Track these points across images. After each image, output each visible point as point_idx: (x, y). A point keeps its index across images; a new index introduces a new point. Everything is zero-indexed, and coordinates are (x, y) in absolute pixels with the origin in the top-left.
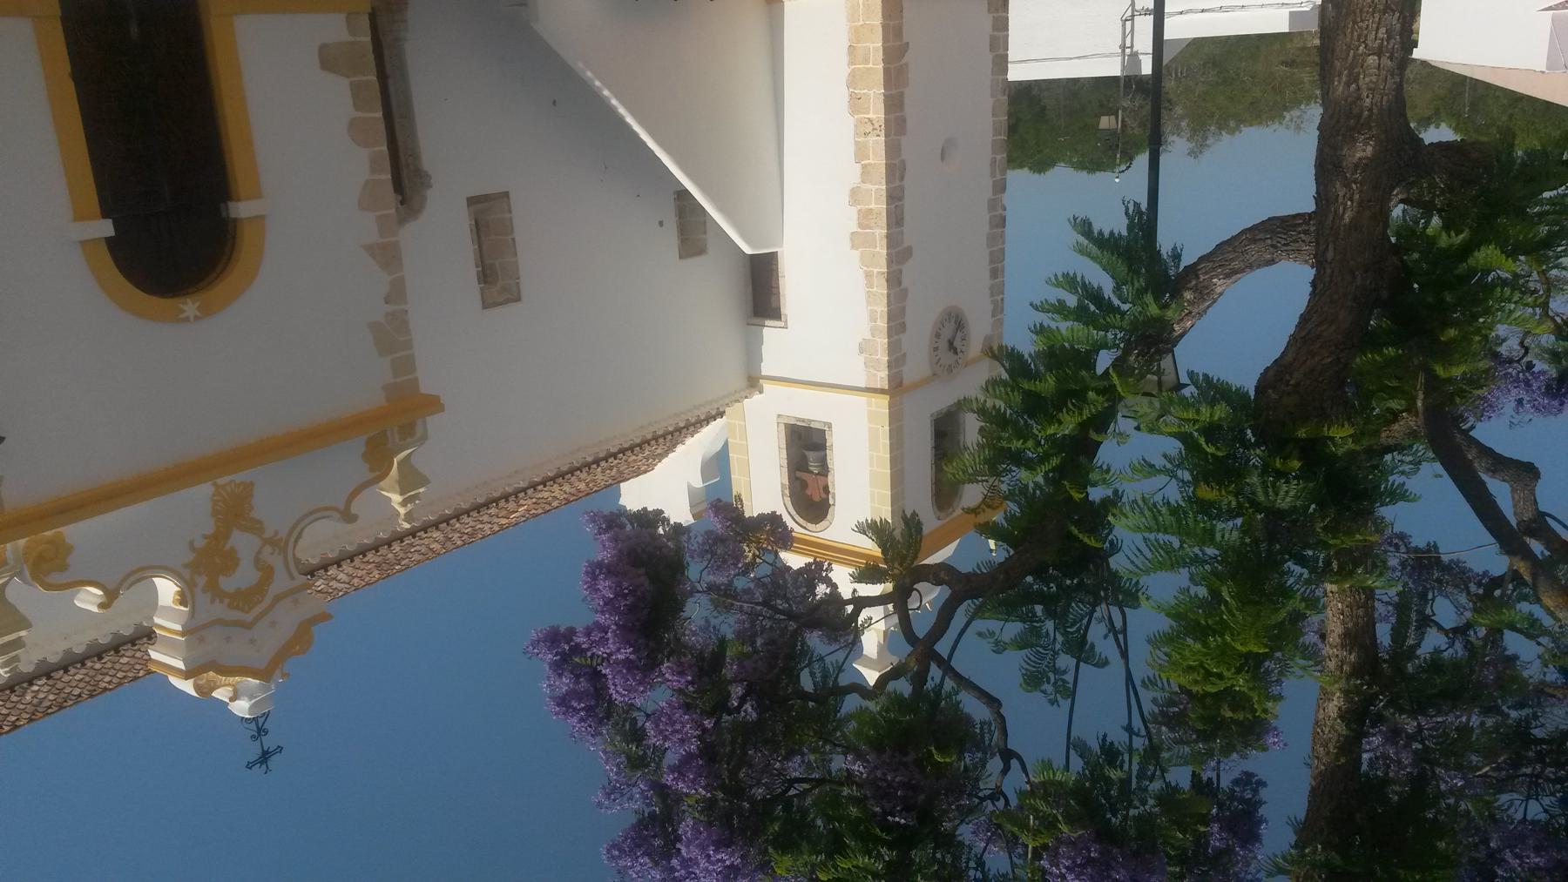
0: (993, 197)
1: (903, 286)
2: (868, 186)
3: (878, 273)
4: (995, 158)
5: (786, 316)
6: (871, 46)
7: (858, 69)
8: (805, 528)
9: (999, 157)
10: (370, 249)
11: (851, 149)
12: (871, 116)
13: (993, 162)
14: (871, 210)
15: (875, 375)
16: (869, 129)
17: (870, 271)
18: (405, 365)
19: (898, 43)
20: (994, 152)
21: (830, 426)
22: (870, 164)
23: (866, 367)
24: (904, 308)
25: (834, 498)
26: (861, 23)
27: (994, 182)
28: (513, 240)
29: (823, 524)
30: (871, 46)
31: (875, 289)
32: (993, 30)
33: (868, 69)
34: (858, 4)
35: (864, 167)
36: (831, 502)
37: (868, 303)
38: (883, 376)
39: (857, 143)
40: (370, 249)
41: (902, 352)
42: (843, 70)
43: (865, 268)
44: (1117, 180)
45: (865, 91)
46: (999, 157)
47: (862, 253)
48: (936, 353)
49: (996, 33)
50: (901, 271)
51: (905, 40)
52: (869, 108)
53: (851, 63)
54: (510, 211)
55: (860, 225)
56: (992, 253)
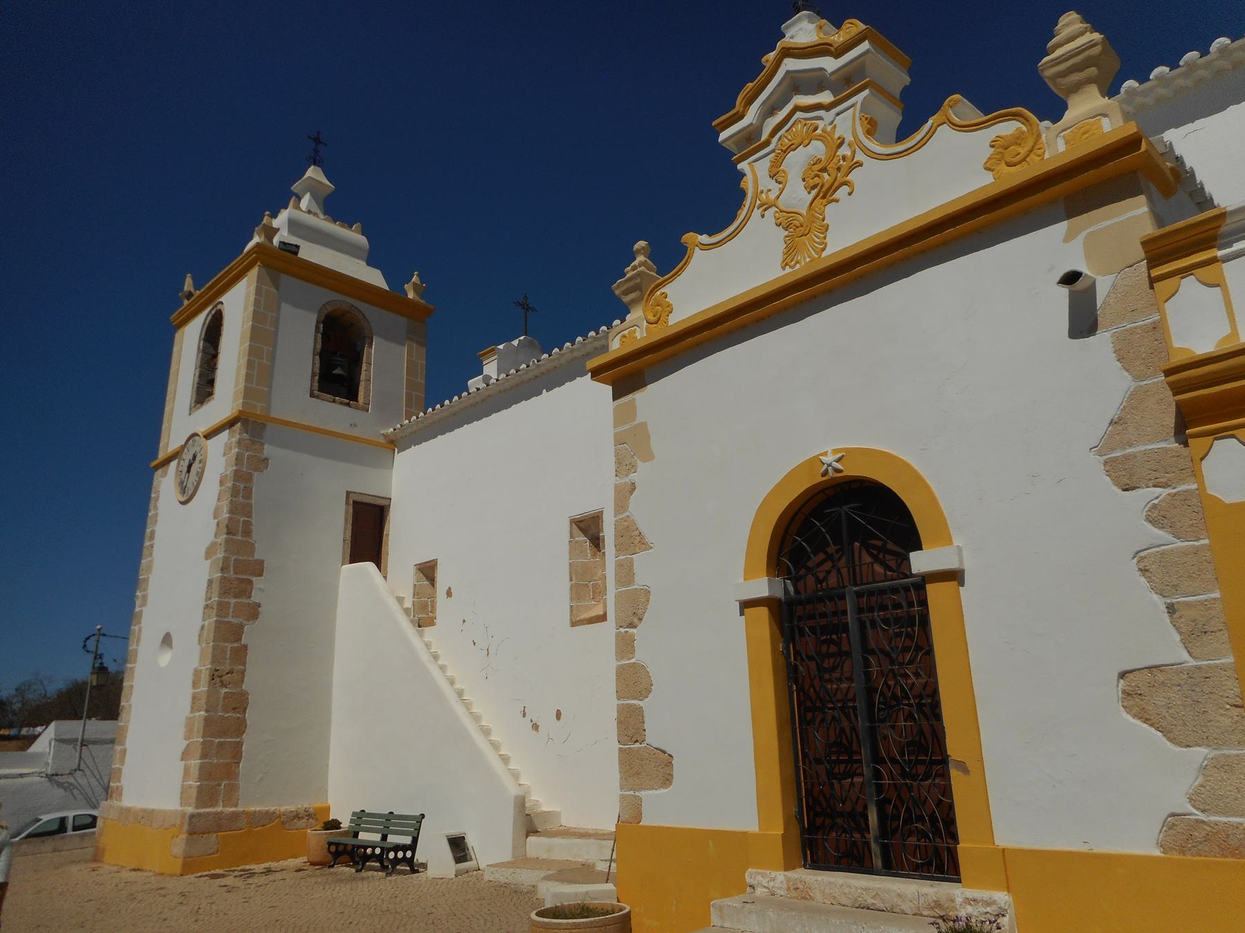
1: (216, 521)
2: (235, 621)
10: (644, 545)
11: (251, 657)
12: (224, 690)
14: (235, 597)
16: (226, 678)
18: (620, 418)
19: (188, 762)
21: (312, 395)
25: (317, 328)
27: (140, 623)
28: (571, 580)
31: (242, 519)
37: (250, 506)
39: (244, 664)
40: (644, 545)
41: (225, 457)
42: (249, 741)
44: (98, 627)
47: (253, 556)
51: (183, 762)
53: (239, 744)
54: (571, 607)
55: (250, 582)
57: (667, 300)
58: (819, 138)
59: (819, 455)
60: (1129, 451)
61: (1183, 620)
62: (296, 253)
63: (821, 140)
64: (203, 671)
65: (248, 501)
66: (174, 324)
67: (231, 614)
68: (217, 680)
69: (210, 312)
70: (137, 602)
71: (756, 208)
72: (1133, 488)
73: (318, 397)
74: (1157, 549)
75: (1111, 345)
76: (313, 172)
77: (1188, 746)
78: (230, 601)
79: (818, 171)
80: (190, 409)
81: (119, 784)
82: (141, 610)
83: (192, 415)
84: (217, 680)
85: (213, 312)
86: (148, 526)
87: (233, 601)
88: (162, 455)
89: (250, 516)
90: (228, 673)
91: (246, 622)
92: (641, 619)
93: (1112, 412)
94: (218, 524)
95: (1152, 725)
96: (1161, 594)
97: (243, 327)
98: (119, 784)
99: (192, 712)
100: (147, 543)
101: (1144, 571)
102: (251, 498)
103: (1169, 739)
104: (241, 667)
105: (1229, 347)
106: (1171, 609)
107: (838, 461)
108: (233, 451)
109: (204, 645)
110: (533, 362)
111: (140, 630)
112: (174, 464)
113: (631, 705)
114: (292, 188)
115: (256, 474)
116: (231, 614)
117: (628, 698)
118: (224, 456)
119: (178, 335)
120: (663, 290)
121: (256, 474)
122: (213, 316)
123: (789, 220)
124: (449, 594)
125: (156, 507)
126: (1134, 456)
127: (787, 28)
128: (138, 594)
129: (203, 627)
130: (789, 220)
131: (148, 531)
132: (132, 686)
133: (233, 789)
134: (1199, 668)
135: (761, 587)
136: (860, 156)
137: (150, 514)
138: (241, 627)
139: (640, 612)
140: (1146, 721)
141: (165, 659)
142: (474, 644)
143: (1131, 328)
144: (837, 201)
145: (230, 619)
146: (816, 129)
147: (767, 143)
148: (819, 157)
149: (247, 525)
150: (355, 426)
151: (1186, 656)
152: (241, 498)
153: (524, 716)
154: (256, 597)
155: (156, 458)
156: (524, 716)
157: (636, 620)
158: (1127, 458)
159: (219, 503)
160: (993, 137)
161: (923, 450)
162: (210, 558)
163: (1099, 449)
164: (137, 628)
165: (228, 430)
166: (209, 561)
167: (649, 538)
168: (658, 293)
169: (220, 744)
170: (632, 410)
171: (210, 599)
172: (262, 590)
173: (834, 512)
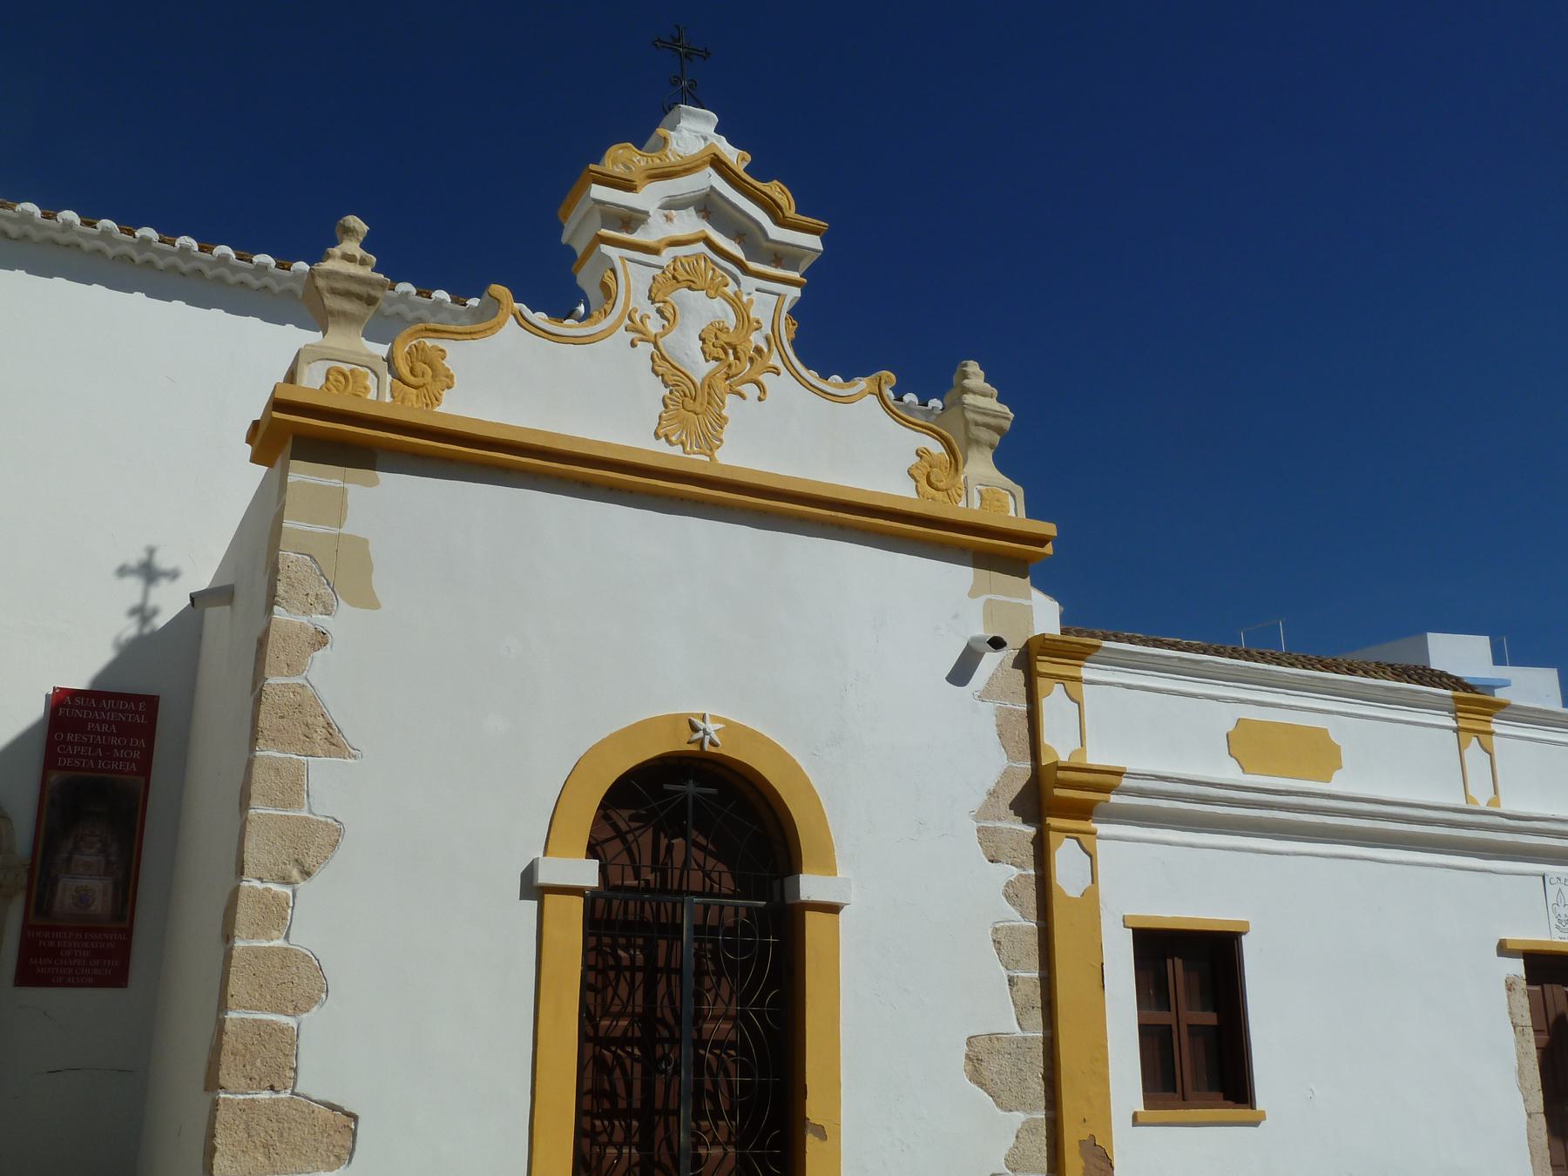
57: (444, 362)
58: (726, 298)
59: (692, 715)
60: (998, 824)
61: (1019, 993)
63: (732, 306)
71: (622, 328)
72: (997, 861)
74: (1007, 924)
75: (994, 718)
77: (1011, 1111)
79: (726, 343)
92: (306, 874)
93: (991, 785)
95: (986, 1090)
96: (1006, 967)
101: (997, 942)
103: (998, 1105)
105: (1075, 762)
106: (1011, 981)
107: (717, 731)
113: (268, 1023)
117: (259, 1009)
120: (441, 344)
123: (676, 378)
126: (1001, 831)
127: (689, 113)
130: (676, 378)
134: (1025, 1039)
135: (588, 874)
136: (775, 360)
139: (309, 862)
140: (981, 1085)
143: (1010, 709)
144: (742, 396)
146: (726, 285)
147: (655, 251)
148: (727, 325)
151: (1017, 1028)
157: (295, 873)
158: (996, 830)
160: (920, 446)
161: (815, 755)
163: (980, 815)
167: (351, 735)
168: (429, 343)
170: (337, 508)
173: (676, 792)
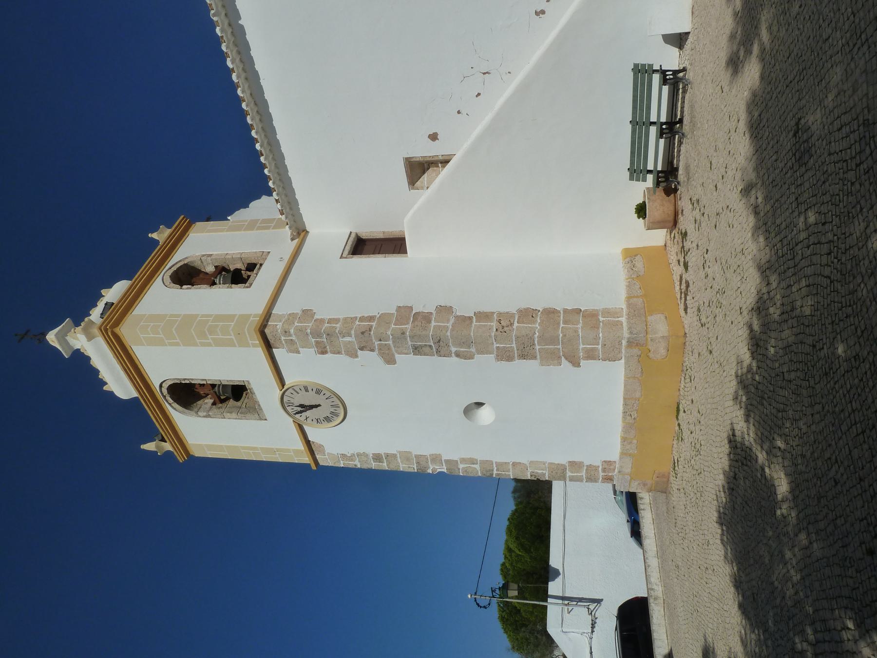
0: (443, 459)
1: (360, 352)
2: (452, 320)
3: (372, 326)
4: (477, 464)
5: (352, 258)
6: (580, 326)
7: (559, 316)
8: (170, 268)
9: (477, 467)
12: (516, 324)
13: (473, 461)
14: (429, 322)
15: (280, 321)
17: (374, 320)
20: (483, 462)
22: (472, 322)
23: (290, 314)
24: (339, 353)
25: (187, 288)
26: (601, 319)
29: (168, 280)
30: (580, 326)
31: (357, 323)
32: (587, 466)
33: (559, 324)
34: (618, 317)
35: (470, 318)
36: (184, 287)
37: (345, 319)
38: (278, 327)
39: (493, 313)
41: (300, 349)
43: (378, 316)
44: (469, 596)
45: (539, 321)
46: (477, 467)
48: (303, 389)
49: (585, 467)
50: (372, 350)
51: (582, 362)
52: (523, 323)
53: (565, 311)
55: (417, 314)
56: (394, 456)
62: (113, 304)
64: (498, 345)
65: (341, 321)
66: (186, 459)
67: (446, 324)
68: (506, 329)
69: (170, 404)
70: (439, 470)
73: (251, 285)
76: (51, 337)
78: (433, 325)
80: (261, 419)
81: (600, 469)
82: (447, 461)
83: (267, 417)
84: (506, 329)
85: (171, 401)
86: (369, 467)
87: (433, 324)
88: (306, 459)
89: (356, 318)
90: (501, 324)
91: (454, 314)
94: (362, 349)
97: (177, 344)
98: (600, 469)
99: (535, 358)
100: (384, 466)
102: (339, 319)
104: (495, 315)
108: (294, 338)
109: (473, 350)
110: (214, 15)
111: (463, 460)
112: (313, 434)
114: (67, 357)
115: (316, 317)
116: (446, 324)
118: (298, 352)
119: (197, 453)
121: (316, 317)
122: (175, 401)
124: (434, 137)
125: (351, 458)
128: (430, 471)
129: (458, 355)
131: (374, 465)
132: (514, 464)
133: (607, 312)
137: (359, 466)
138: (457, 317)
141: (485, 415)
142: (479, 94)
145: (450, 325)
149: (362, 319)
150: (281, 258)
152: (338, 325)
153: (543, 12)
154: (431, 309)
155: (308, 465)
156: (543, 12)
159: (343, 353)
162: (393, 355)
164: (461, 466)
165: (274, 349)
166: (397, 356)
169: (565, 322)
171: (430, 346)
172: (424, 306)
